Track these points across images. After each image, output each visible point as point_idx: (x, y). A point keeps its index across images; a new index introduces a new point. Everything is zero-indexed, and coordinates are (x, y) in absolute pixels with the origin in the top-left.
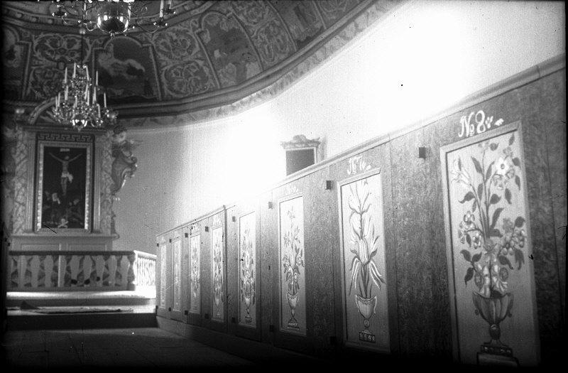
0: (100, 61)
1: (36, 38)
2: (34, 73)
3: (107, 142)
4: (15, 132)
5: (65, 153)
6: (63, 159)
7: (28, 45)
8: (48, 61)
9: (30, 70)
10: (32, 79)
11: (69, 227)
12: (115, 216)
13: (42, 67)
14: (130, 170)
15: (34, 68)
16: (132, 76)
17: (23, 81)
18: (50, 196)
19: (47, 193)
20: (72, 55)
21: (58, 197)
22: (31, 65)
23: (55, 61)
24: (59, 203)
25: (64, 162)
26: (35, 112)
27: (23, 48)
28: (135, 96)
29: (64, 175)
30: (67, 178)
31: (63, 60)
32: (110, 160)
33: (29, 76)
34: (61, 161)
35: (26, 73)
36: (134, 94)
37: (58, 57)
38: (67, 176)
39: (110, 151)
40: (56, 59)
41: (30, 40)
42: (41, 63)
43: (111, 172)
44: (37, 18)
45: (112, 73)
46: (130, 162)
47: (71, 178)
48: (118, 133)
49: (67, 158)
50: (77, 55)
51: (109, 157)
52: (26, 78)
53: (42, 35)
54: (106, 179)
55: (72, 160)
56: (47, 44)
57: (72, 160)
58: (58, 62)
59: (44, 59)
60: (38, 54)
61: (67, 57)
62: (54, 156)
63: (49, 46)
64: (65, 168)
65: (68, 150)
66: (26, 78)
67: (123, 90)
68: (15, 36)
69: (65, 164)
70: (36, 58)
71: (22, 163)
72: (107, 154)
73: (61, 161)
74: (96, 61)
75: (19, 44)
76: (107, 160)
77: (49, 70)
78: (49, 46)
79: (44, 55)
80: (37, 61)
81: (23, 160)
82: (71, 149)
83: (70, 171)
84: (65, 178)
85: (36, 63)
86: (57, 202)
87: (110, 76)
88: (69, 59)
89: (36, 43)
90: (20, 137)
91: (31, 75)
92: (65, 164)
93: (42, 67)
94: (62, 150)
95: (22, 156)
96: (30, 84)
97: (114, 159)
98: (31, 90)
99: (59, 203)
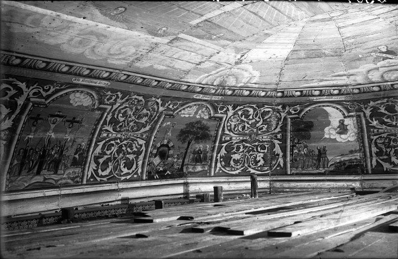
1: (366, 108)
7: (359, 116)
9: (370, 140)
10: (374, 149)
13: (383, 135)
15: (375, 137)
27: (355, 118)
35: (367, 145)
41: (360, 110)
44: (359, 89)
52: (368, 150)
53: (372, 103)
56: (383, 110)
59: (384, 127)
63: (386, 112)
68: (341, 111)
70: (374, 127)
75: (349, 117)
77: (393, 137)
78: (386, 112)
79: (382, 123)
80: (375, 130)
89: (368, 112)
91: (373, 145)
93: (383, 135)
96: (374, 155)
98: (377, 161)
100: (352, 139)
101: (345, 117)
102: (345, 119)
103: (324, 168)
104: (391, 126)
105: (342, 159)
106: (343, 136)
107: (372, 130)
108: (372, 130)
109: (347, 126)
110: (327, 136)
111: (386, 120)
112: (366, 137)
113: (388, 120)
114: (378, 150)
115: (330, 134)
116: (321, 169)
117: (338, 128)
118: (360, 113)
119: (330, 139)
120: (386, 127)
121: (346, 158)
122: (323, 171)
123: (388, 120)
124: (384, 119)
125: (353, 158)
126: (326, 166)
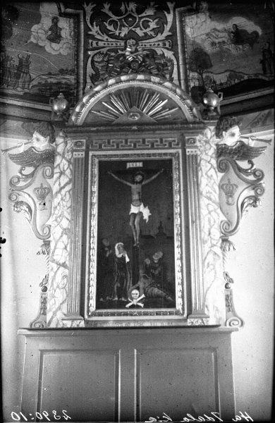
0: (188, 30)
2: (93, 62)
3: (208, 146)
4: (52, 140)
5: (134, 171)
6: (134, 182)
8: (110, 40)
9: (86, 57)
10: (90, 71)
11: (146, 306)
12: (231, 281)
13: (102, 50)
14: (252, 193)
16: (241, 47)
17: (78, 75)
18: (112, 247)
19: (106, 243)
20: (146, 25)
21: (126, 248)
22: (86, 50)
23: (122, 39)
24: (127, 260)
25: (134, 187)
26: (83, 106)
28: (248, 80)
29: (134, 210)
30: (141, 213)
31: (132, 35)
32: (215, 176)
33: (85, 68)
34: (128, 184)
36: (246, 77)
37: (124, 32)
38: (140, 210)
39: (214, 162)
40: (122, 35)
42: (101, 44)
43: (218, 200)
45: (208, 49)
46: (251, 178)
47: (146, 213)
48: (226, 130)
49: (138, 178)
50: (153, 25)
51: (212, 172)
52: (82, 72)
54: (210, 213)
55: (147, 181)
57: (147, 181)
58: (126, 39)
60: (95, 30)
61: (138, 31)
62: (116, 178)
64: (136, 197)
65: (140, 165)
66: (82, 72)
67: (228, 74)
69: (135, 188)
70: (93, 37)
71: (63, 192)
72: (209, 166)
73: (128, 184)
74: (183, 32)
76: (210, 177)
77: (113, 54)
78: (110, 14)
79: (104, 31)
80: (94, 42)
81: (64, 187)
82: (145, 162)
83: (145, 200)
84: (135, 215)
85: (94, 45)
86: (123, 258)
87: (206, 54)
88: (140, 32)
90: (60, 149)
92: (135, 188)
93: (102, 50)
94: (129, 165)
95: (64, 180)
96: (89, 80)
97: (220, 175)
99: (127, 260)
100: (64, 52)
101: (61, 14)
102: (60, 18)
103: (23, 88)
104: (113, 36)
105: (49, 80)
106: (54, 45)
107: (90, 41)
108: (90, 41)
109: (61, 29)
110: (32, 40)
111: (109, 28)
112: (82, 52)
113: (111, 28)
114: (94, 73)
115: (38, 38)
116: (19, 89)
117: (50, 29)
118: (78, 11)
119: (37, 45)
120: (107, 37)
121: (54, 81)
122: (22, 93)
123: (111, 28)
124: (107, 24)
125: (64, 81)
126: (26, 86)
